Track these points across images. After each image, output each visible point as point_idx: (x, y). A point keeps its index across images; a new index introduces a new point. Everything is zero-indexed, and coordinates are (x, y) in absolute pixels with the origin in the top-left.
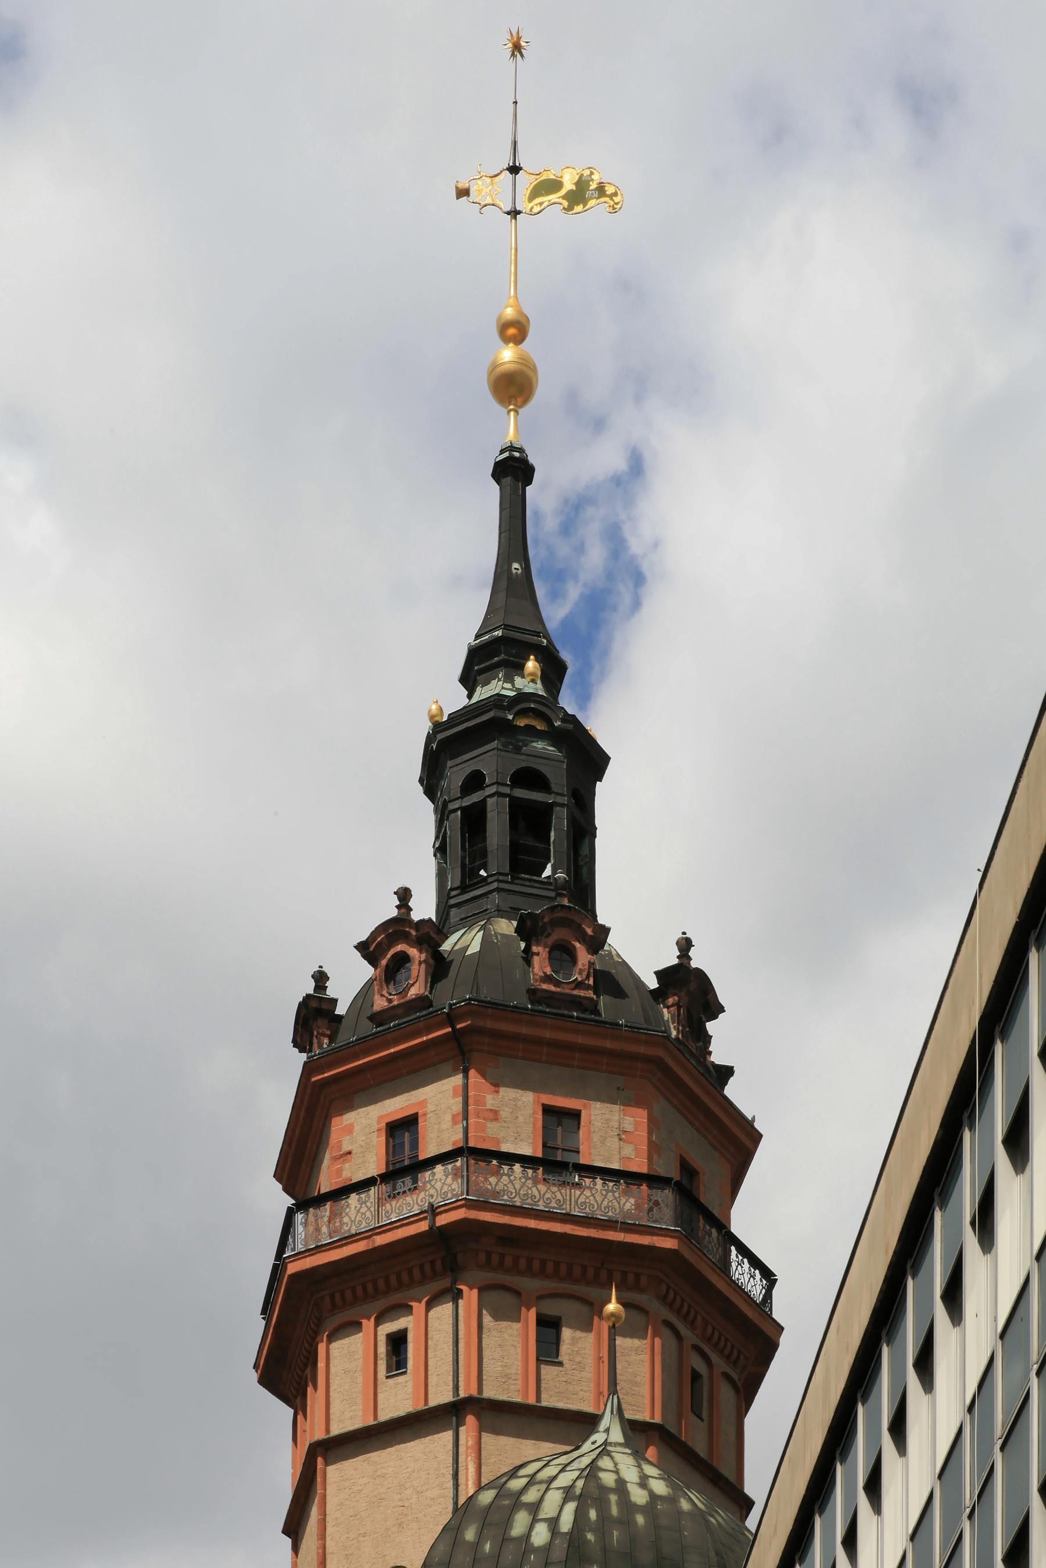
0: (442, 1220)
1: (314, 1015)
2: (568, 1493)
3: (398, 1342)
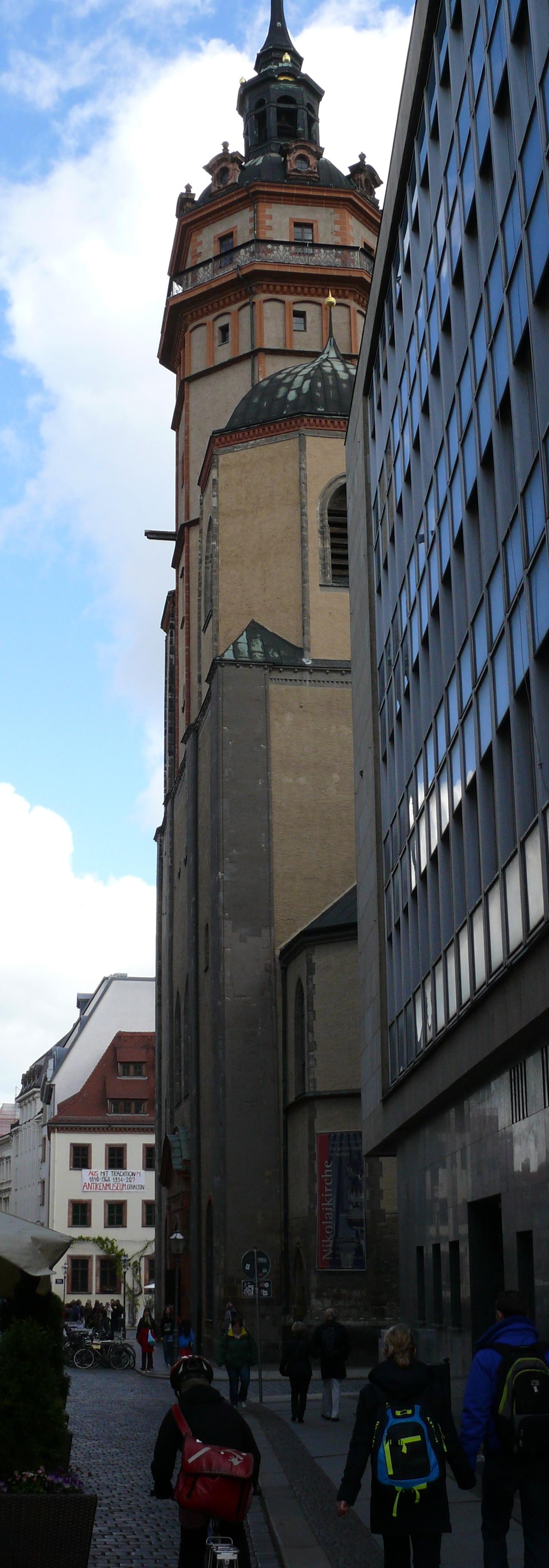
0: (245, 272)
1: (185, 202)
2: (306, 377)
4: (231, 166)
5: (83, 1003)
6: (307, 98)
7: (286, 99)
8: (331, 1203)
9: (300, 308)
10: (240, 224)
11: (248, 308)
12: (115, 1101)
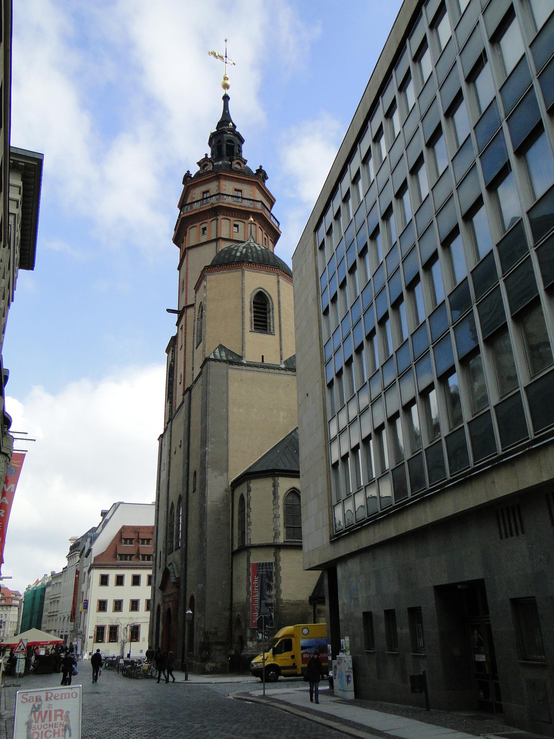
0: (215, 206)
1: (187, 176)
2: (244, 247)
3: (204, 229)
4: (209, 163)
5: (104, 514)
6: (238, 142)
7: (230, 141)
8: (258, 595)
9: (236, 223)
10: (213, 187)
11: (215, 221)
12: (121, 555)
